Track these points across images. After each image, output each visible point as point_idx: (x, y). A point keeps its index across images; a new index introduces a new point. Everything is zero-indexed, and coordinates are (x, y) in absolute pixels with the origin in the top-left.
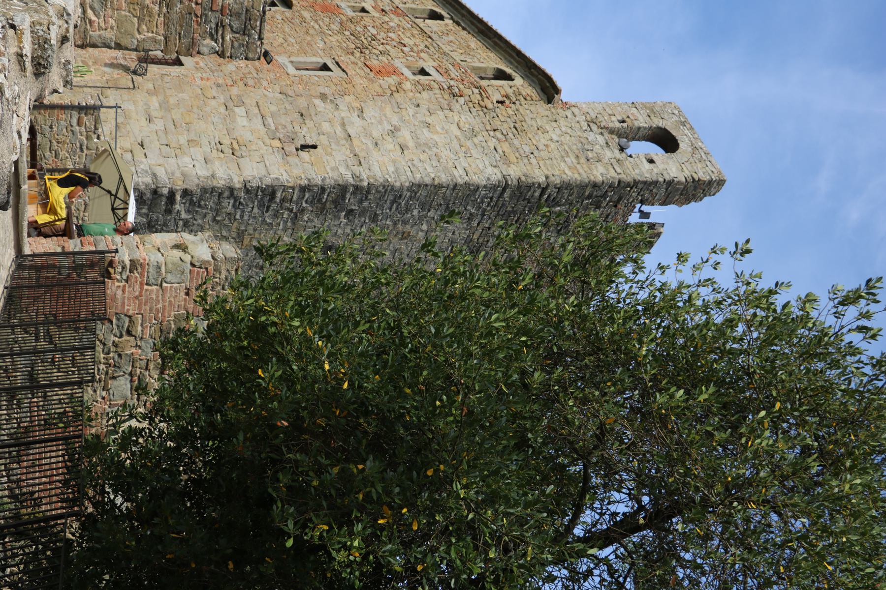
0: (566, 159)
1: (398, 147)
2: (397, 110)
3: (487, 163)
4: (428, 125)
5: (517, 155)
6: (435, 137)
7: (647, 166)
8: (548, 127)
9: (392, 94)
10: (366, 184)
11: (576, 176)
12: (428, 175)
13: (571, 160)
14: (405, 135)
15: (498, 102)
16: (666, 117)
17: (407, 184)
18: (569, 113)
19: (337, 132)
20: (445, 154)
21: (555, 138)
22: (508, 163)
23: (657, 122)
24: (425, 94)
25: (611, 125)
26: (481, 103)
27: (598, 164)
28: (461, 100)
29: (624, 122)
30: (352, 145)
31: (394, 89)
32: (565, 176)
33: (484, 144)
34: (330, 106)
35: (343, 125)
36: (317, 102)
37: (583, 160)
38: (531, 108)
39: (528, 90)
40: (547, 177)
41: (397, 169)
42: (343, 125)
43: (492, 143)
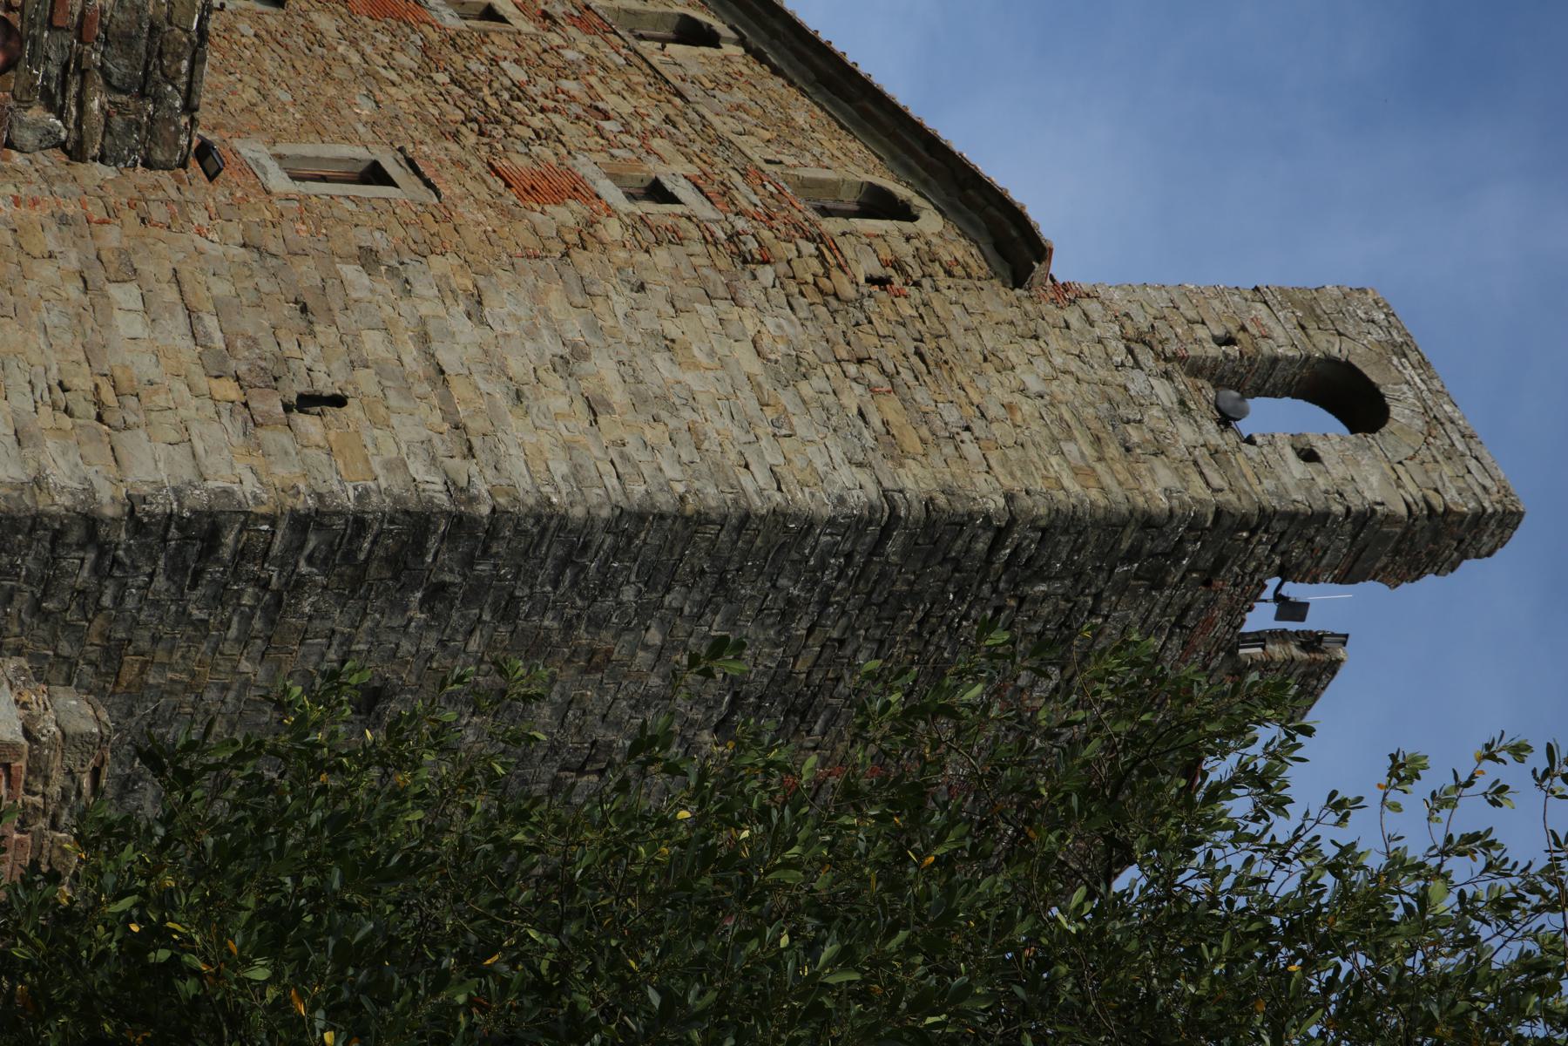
0: (1067, 447)
1: (580, 405)
2: (579, 299)
3: (837, 455)
4: (670, 344)
5: (924, 432)
6: (689, 377)
7: (1298, 468)
8: (1012, 355)
9: (566, 254)
10: (485, 510)
11: (1094, 494)
12: (667, 486)
14: (603, 370)
15: (871, 280)
17: (605, 513)
19: (406, 359)
20: (717, 426)
21: (1034, 385)
22: (899, 456)
24: (662, 256)
25: (1194, 351)
26: (824, 283)
27: (1157, 463)
28: (766, 274)
29: (1229, 341)
30: (447, 398)
31: (572, 238)
32: (1061, 495)
33: (830, 400)
34: (385, 286)
35: (424, 339)
36: (350, 271)
37: (1113, 451)
38: (969, 300)
39: (958, 249)
40: (1010, 497)
41: (576, 469)
42: (424, 339)
43: (853, 397)
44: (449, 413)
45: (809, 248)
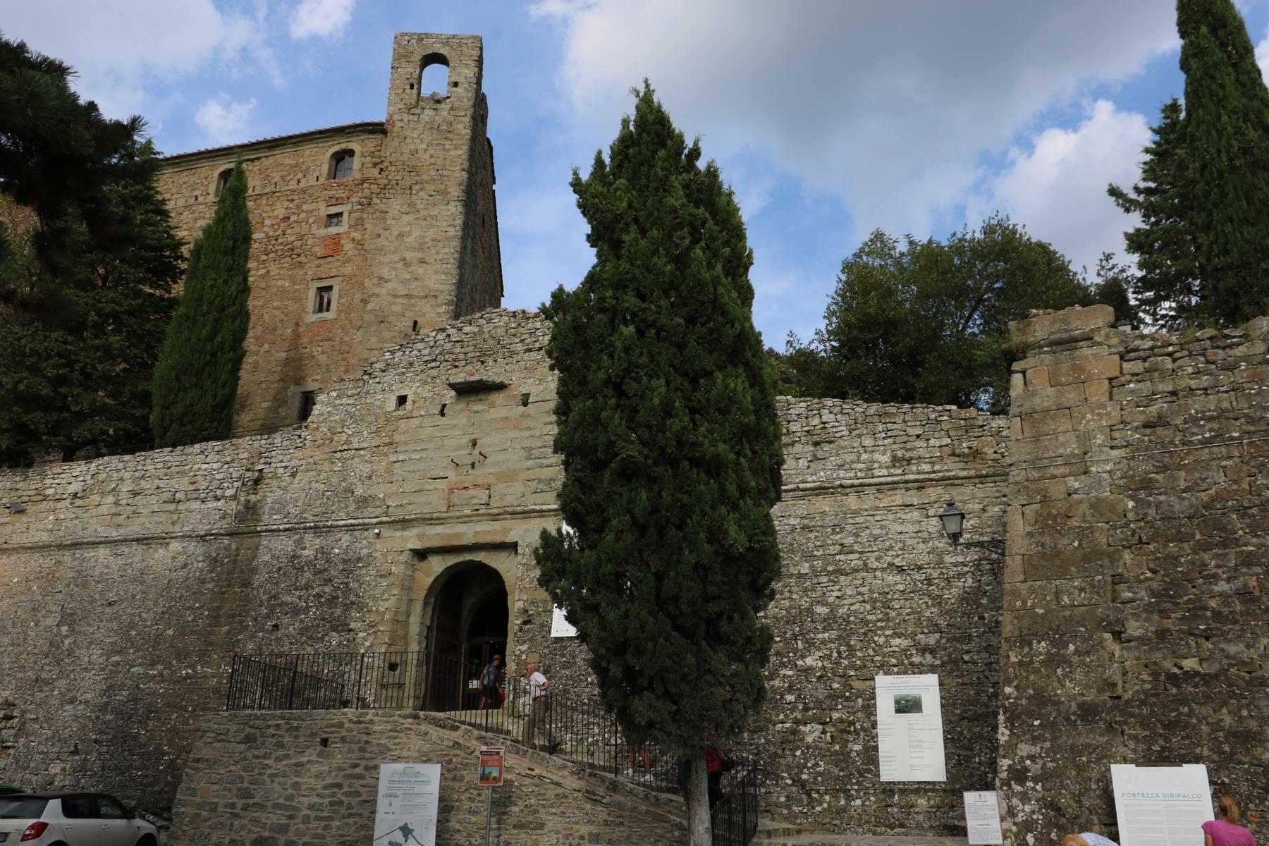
4: (401, 235)
7: (459, 89)
13: (448, 145)
14: (408, 255)
16: (411, 49)
18: (399, 124)
20: (431, 233)
21: (424, 146)
22: (444, 193)
23: (417, 57)
25: (415, 96)
28: (375, 200)
35: (395, 296)
36: (369, 307)
37: (450, 136)
42: (395, 296)
44: (422, 298)
45: (366, 185)
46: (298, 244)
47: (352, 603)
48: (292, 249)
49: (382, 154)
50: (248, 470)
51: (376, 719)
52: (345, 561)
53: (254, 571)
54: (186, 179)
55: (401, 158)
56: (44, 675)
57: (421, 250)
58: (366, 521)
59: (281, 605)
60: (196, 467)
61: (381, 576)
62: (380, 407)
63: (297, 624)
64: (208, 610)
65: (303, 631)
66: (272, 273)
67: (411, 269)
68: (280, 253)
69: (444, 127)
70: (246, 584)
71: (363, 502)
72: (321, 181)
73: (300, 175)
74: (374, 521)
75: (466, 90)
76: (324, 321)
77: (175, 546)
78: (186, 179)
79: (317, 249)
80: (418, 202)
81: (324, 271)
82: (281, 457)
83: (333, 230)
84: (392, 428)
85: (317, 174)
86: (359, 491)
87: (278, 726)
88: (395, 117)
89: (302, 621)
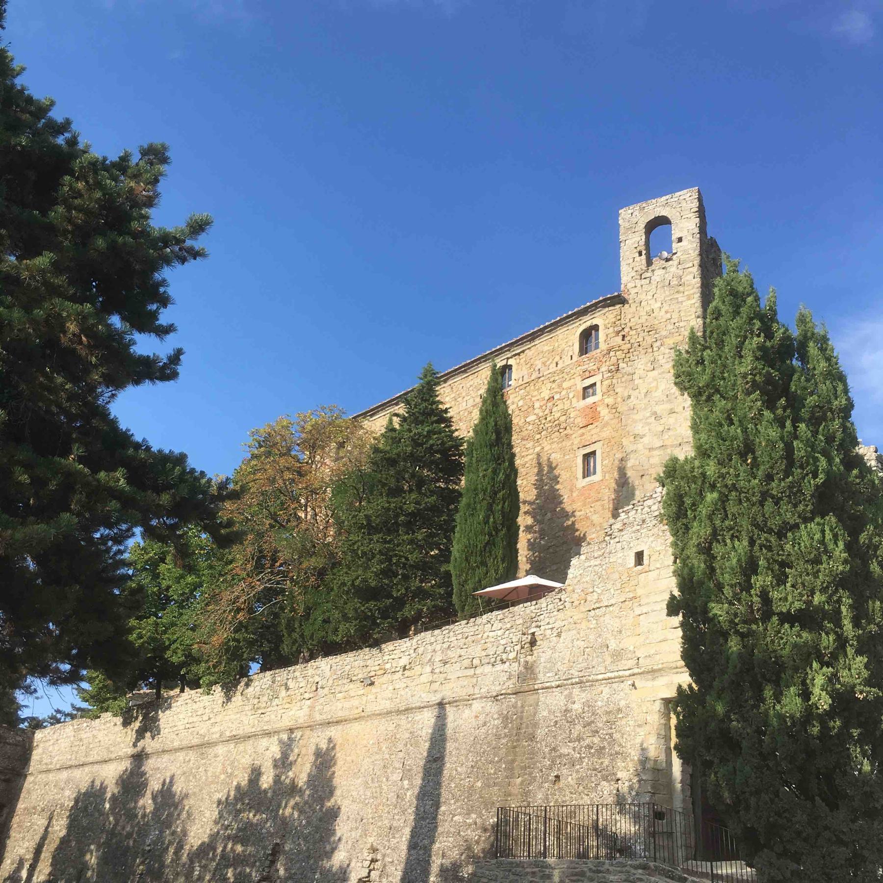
0: (680, 300)
2: (635, 411)
8: (648, 309)
14: (659, 409)
15: (623, 340)
16: (635, 220)
18: (633, 291)
25: (644, 262)
28: (622, 365)
31: (614, 411)
32: (697, 305)
33: (666, 356)
37: (681, 288)
40: (698, 317)
45: (612, 354)
46: (563, 418)
47: (617, 753)
48: (560, 425)
49: (623, 321)
50: (524, 634)
51: (611, 868)
52: (608, 713)
53: (535, 725)
54: (471, 383)
55: (640, 321)
56: (395, 824)
57: (670, 401)
58: (621, 673)
59: (560, 756)
60: (485, 635)
61: (639, 726)
62: (621, 565)
63: (574, 775)
64: (505, 763)
65: (580, 781)
66: (546, 449)
67: (662, 421)
68: (550, 430)
69: (675, 282)
70: (532, 738)
71: (617, 655)
72: (575, 358)
73: (557, 358)
74: (628, 673)
75: (691, 242)
76: (591, 485)
77: (477, 706)
78: (471, 383)
79: (579, 420)
80: (661, 357)
81: (588, 438)
82: (547, 620)
83: (590, 400)
84: (633, 583)
85: (570, 353)
86: (613, 645)
87: (534, 873)
88: (630, 285)
89: (577, 771)
